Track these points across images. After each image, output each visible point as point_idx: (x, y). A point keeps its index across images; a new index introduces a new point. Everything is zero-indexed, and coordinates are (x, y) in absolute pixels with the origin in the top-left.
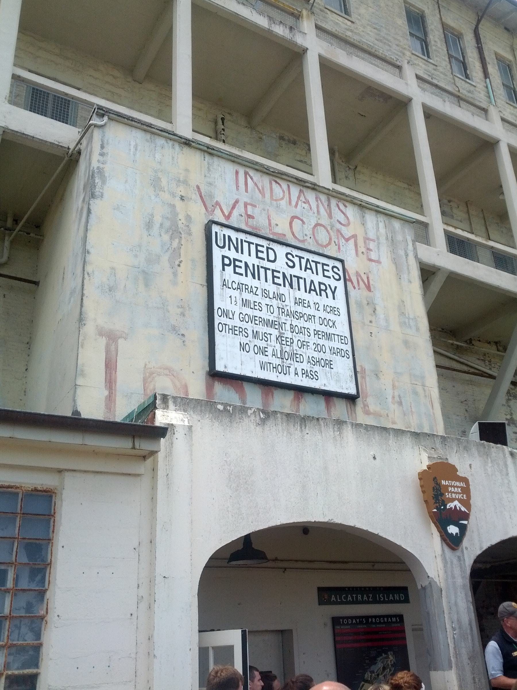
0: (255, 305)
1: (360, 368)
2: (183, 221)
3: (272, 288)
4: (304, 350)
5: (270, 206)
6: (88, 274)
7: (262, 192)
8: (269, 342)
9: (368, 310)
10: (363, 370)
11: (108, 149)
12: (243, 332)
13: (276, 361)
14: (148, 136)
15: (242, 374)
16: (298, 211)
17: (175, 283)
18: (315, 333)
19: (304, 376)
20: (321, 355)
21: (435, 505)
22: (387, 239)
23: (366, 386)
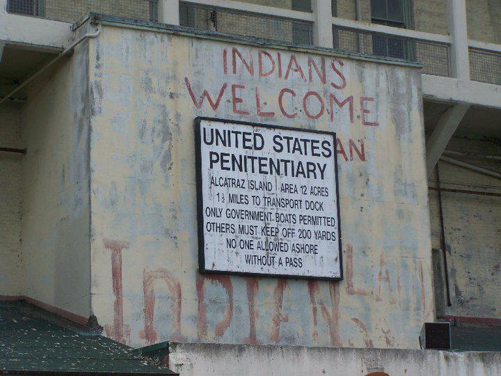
0: (241, 199)
3: (258, 178)
9: (361, 181)
10: (350, 249)
13: (262, 253)
14: (138, 34)
19: (288, 264)
20: (307, 241)
22: (388, 93)
23: (352, 266)
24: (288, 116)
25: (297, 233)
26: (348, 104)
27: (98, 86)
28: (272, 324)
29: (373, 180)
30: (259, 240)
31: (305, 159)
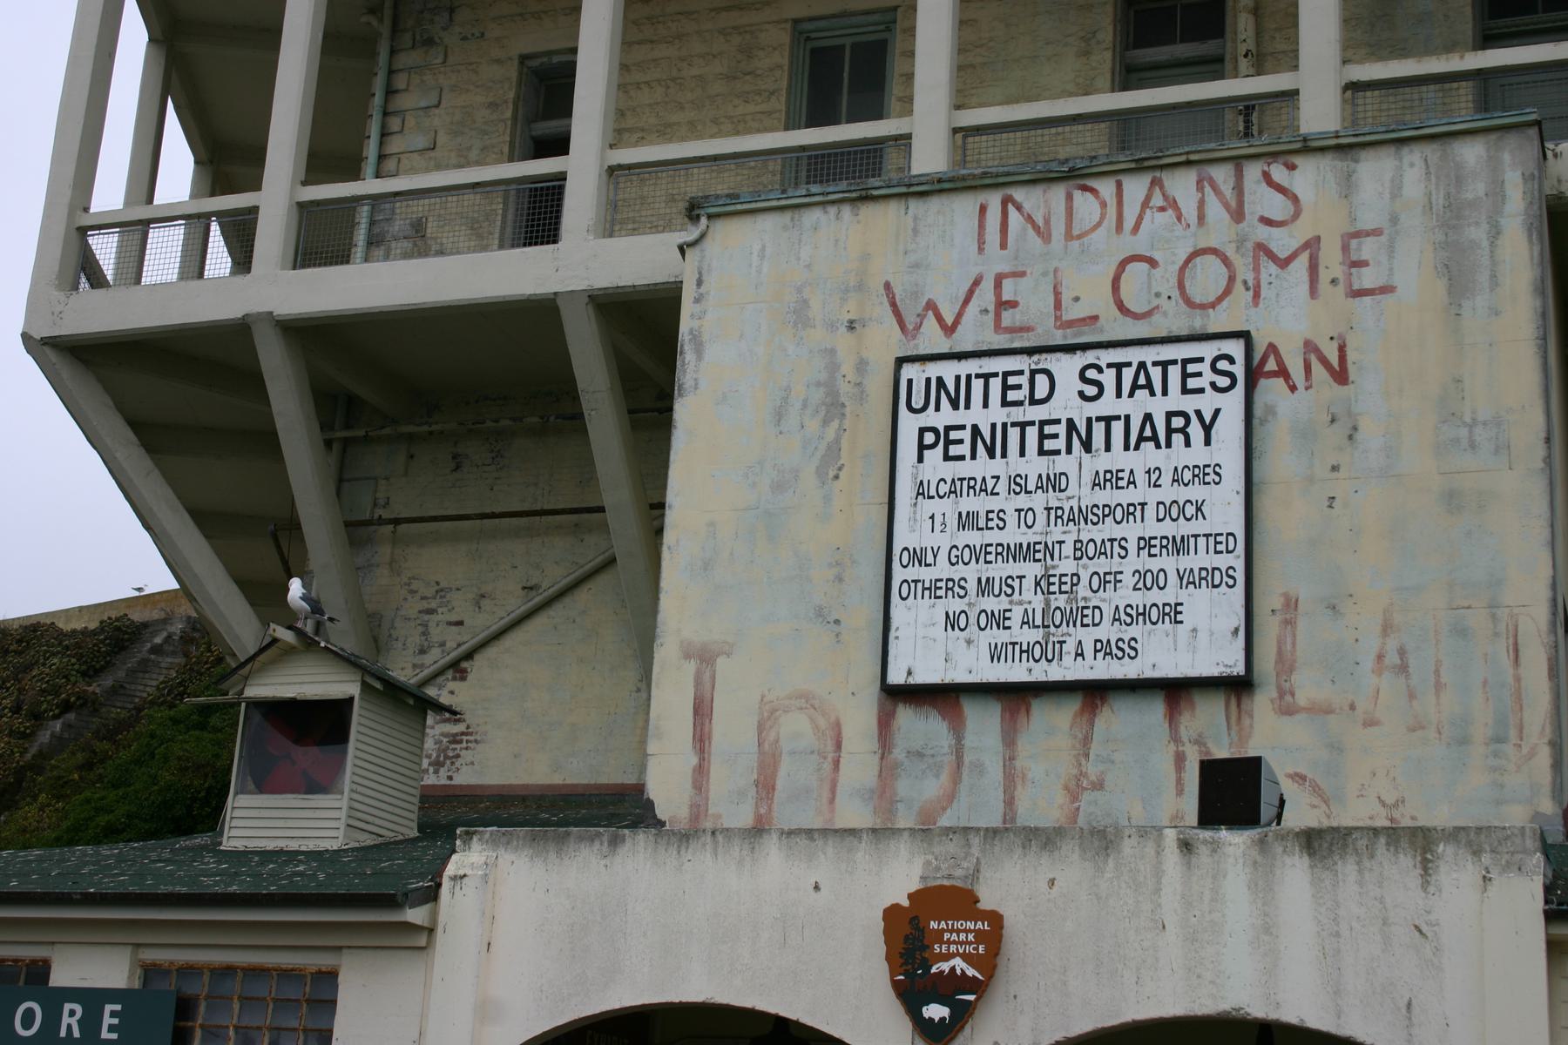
0: (988, 520)
1: (1282, 600)
3: (1034, 466)
6: (669, 548)
7: (1044, 233)
8: (1016, 596)
10: (1291, 604)
11: (710, 284)
12: (956, 589)
13: (1029, 636)
15: (946, 681)
16: (1139, 245)
20: (1155, 596)
21: (905, 967)
23: (1294, 644)
24: (1137, 316)
25: (1128, 580)
26: (1304, 259)
27: (696, 338)
28: (1061, 797)
29: (1371, 434)
30: (1026, 606)
31: (1158, 407)
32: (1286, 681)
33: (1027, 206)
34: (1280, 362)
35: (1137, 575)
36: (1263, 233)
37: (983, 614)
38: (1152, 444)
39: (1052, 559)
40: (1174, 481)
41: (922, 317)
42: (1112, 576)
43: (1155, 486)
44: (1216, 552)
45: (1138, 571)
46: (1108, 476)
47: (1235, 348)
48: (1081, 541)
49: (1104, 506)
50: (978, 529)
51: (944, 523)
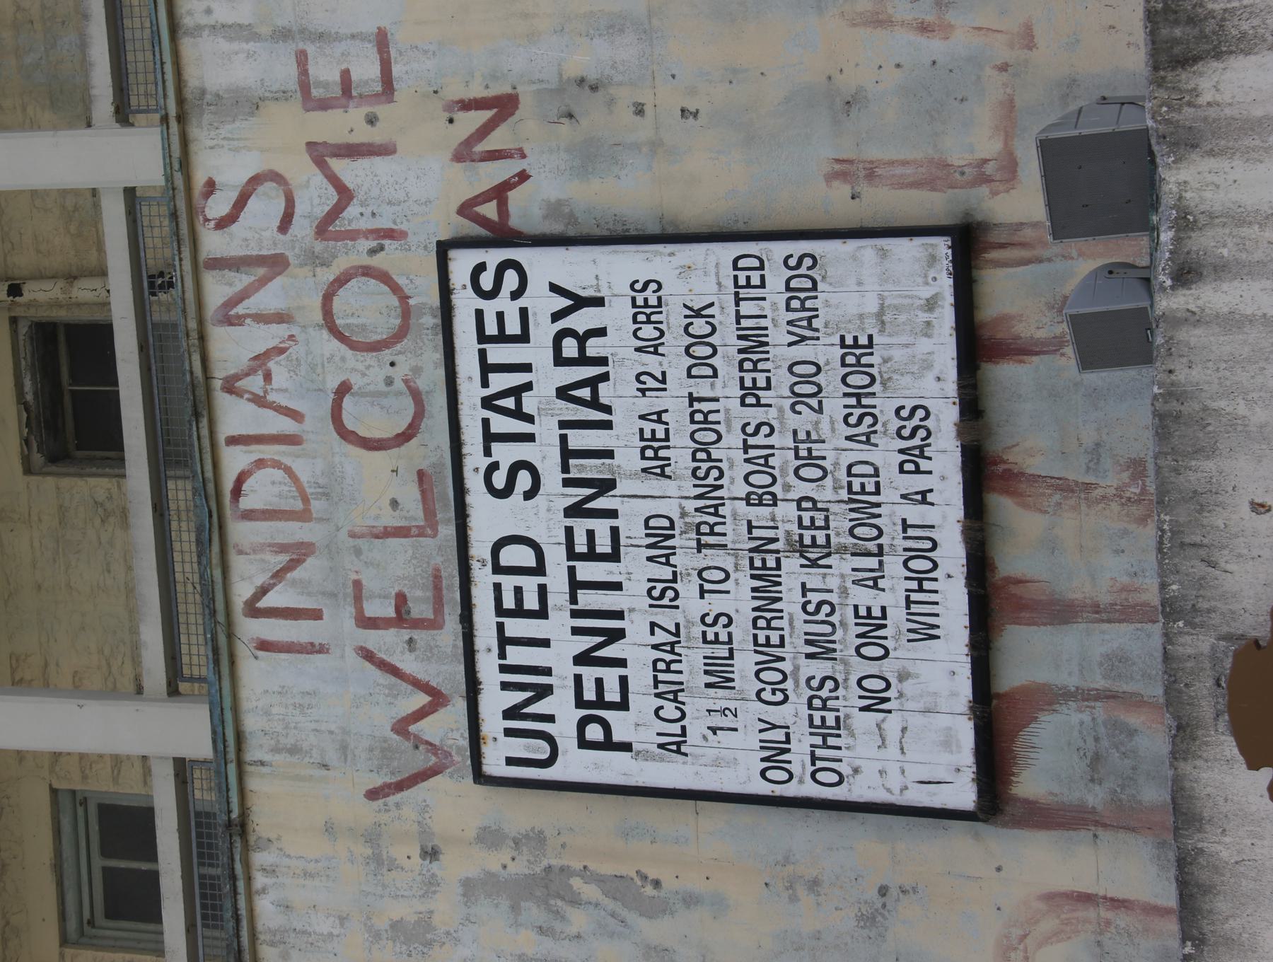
0: (717, 641)
1: (836, 183)
2: (505, 855)
4: (831, 456)
5: (338, 529)
7: (298, 554)
10: (843, 171)
12: (824, 693)
16: (316, 411)
17: (719, 905)
18: (753, 401)
19: (924, 465)
20: (830, 380)
23: (905, 163)
24: (419, 414)
26: (337, 165)
31: (548, 378)
32: (963, 173)
33: (261, 580)
34: (484, 198)
35: (798, 408)
36: (302, 228)
37: (864, 651)
38: (602, 387)
39: (777, 540)
40: (656, 353)
41: (418, 742)
42: (801, 446)
43: (664, 381)
44: (763, 285)
45: (793, 405)
46: (649, 453)
47: (462, 263)
48: (749, 494)
49: (694, 459)
50: (731, 657)
51: (723, 712)
